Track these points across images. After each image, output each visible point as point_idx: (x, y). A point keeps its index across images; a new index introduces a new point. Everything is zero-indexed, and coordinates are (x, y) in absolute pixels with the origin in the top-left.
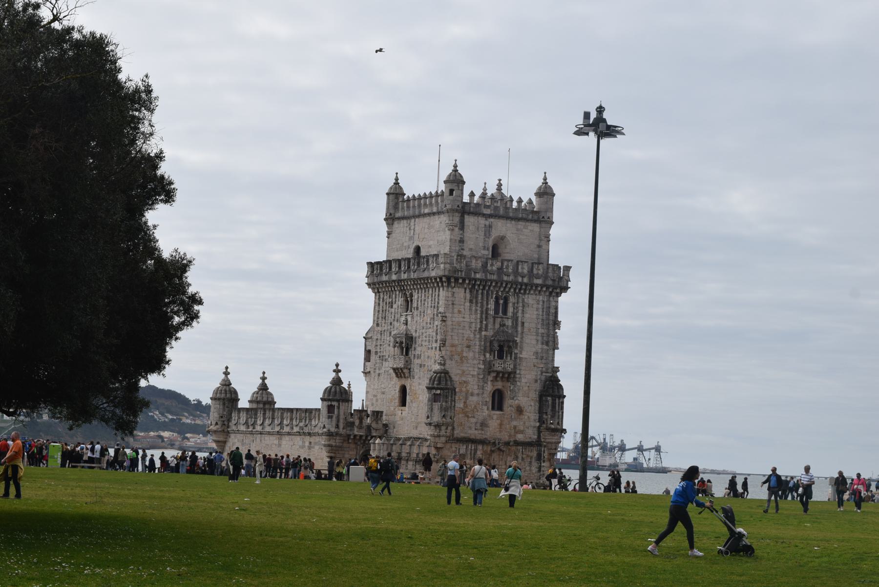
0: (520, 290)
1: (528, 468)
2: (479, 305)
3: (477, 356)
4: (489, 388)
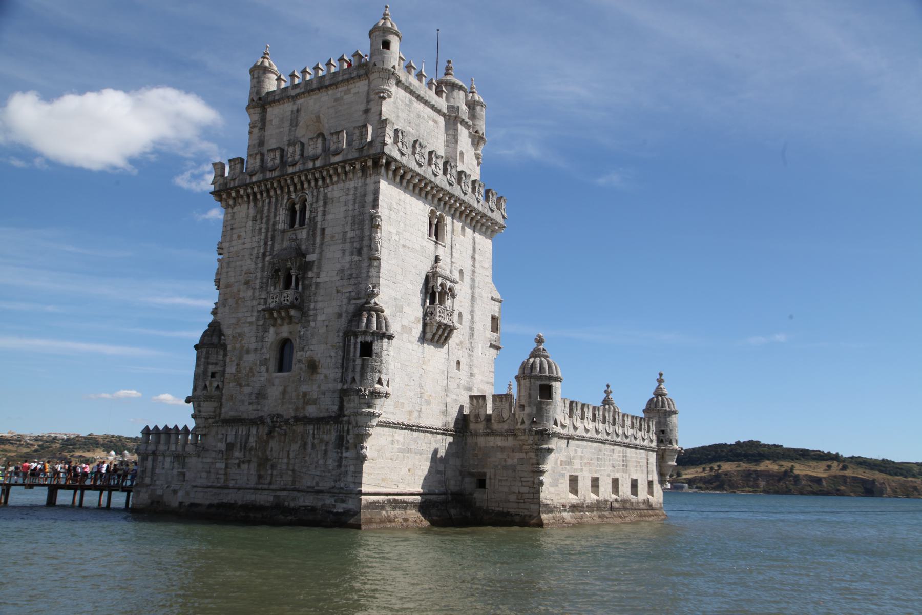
0: (316, 180)
1: (321, 462)
2: (264, 221)
3: (257, 294)
4: (271, 336)
